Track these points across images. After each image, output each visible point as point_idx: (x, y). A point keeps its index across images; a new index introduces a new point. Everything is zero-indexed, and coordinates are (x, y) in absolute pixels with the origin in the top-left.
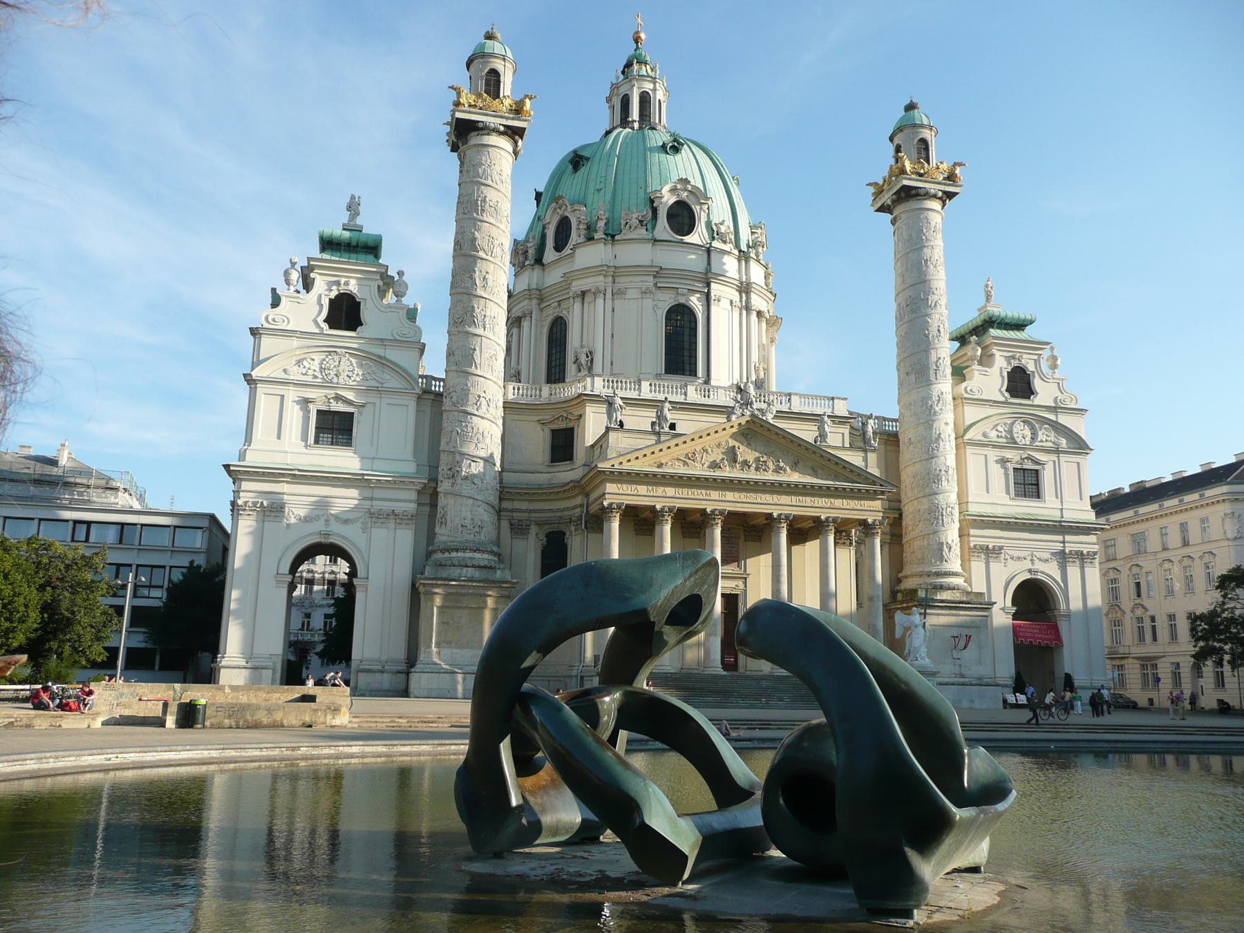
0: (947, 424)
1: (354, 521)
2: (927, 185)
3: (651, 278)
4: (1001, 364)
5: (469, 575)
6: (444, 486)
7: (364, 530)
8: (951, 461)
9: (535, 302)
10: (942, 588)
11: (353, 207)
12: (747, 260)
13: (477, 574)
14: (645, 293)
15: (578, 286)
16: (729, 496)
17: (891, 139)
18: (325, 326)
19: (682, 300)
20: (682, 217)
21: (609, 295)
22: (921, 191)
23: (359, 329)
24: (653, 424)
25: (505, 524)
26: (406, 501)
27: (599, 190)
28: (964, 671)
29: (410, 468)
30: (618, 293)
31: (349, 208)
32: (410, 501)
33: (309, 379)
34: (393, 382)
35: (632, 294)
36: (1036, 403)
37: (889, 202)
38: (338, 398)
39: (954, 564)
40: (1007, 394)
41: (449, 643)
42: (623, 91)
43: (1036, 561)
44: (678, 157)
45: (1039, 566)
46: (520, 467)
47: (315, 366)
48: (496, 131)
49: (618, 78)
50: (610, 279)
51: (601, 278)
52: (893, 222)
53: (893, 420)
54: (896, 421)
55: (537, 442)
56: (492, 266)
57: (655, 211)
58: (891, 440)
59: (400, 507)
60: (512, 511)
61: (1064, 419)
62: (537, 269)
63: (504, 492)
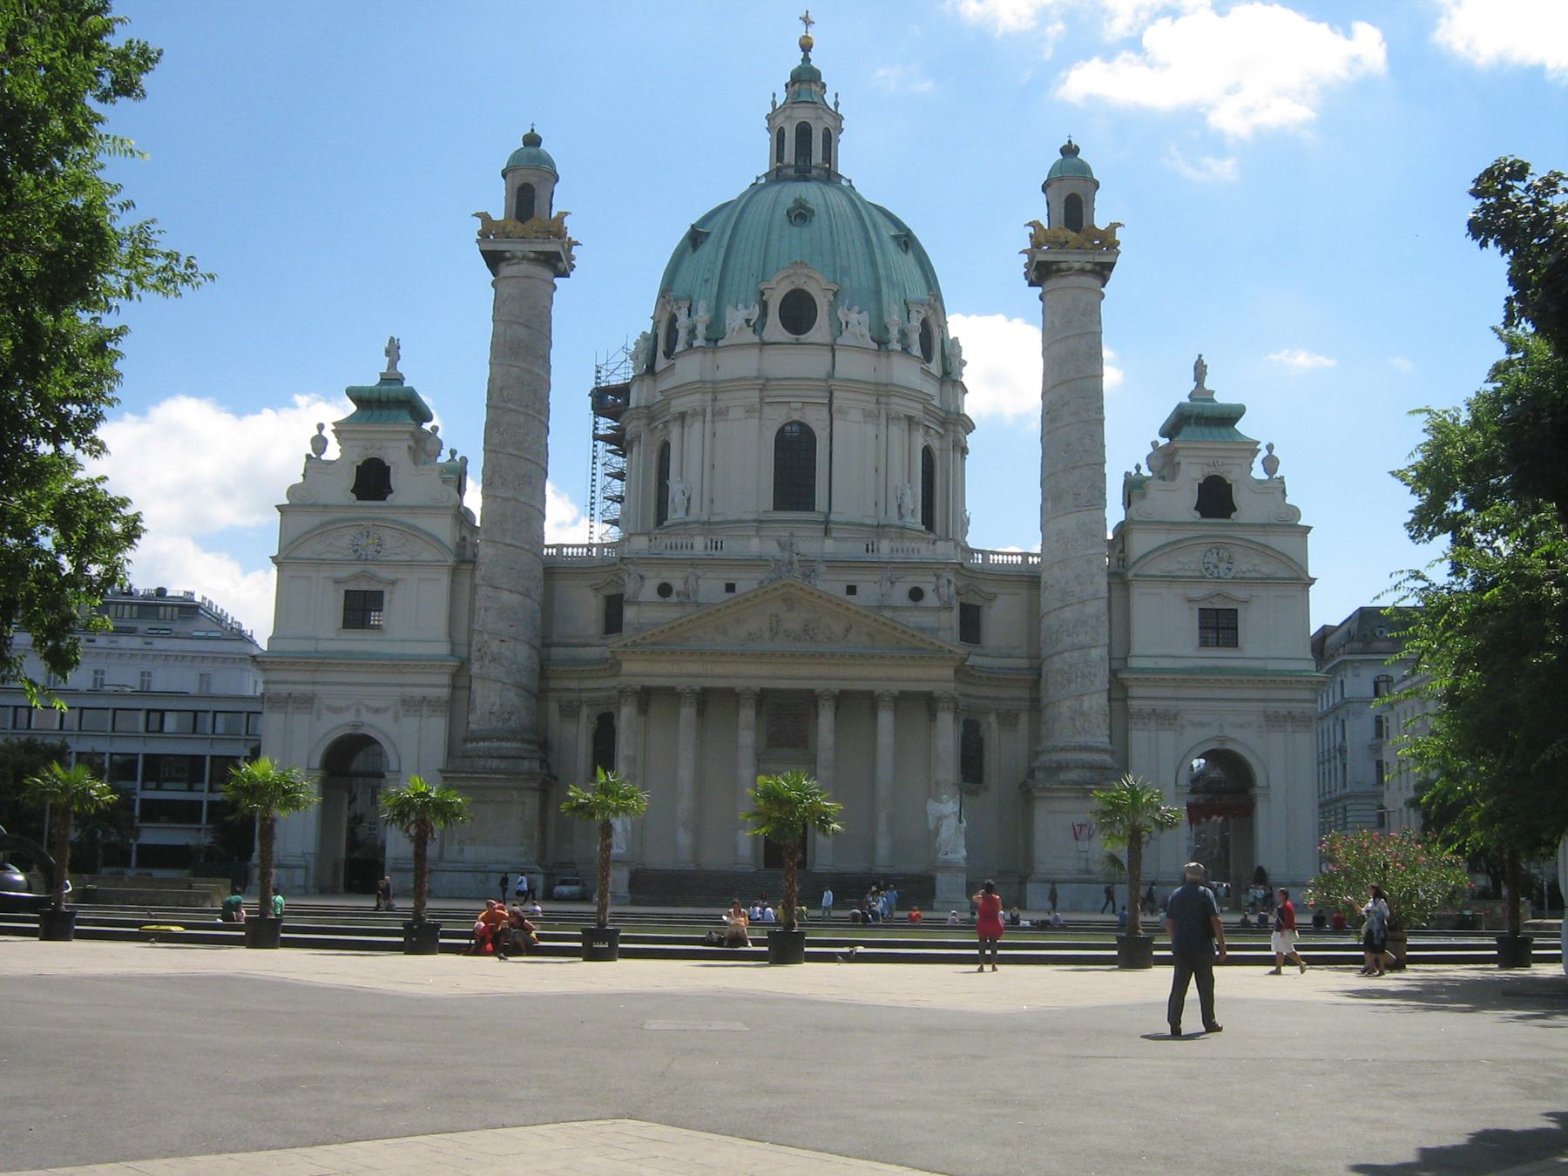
0: (1089, 562)
1: (386, 710)
2: (1069, 258)
3: (757, 393)
4: (1192, 475)
6: (475, 668)
7: (396, 719)
8: (1097, 607)
9: (643, 422)
11: (393, 351)
13: (503, 765)
14: (749, 411)
15: (678, 405)
16: (765, 670)
17: (1044, 189)
18: (354, 497)
19: (796, 416)
20: (798, 312)
21: (708, 417)
22: (1063, 266)
23: (390, 497)
25: (553, 707)
26: (437, 686)
27: (706, 281)
29: (443, 649)
30: (720, 414)
31: (388, 353)
32: (443, 686)
33: (338, 556)
34: (428, 554)
35: (736, 413)
39: (1101, 738)
40: (1198, 514)
42: (779, 122)
45: (1228, 732)
46: (574, 641)
47: (345, 542)
48: (525, 258)
49: (774, 103)
50: (709, 397)
51: (698, 396)
52: (1041, 298)
53: (1033, 555)
54: (1038, 555)
55: (585, 610)
56: (522, 418)
57: (764, 306)
62: (648, 381)
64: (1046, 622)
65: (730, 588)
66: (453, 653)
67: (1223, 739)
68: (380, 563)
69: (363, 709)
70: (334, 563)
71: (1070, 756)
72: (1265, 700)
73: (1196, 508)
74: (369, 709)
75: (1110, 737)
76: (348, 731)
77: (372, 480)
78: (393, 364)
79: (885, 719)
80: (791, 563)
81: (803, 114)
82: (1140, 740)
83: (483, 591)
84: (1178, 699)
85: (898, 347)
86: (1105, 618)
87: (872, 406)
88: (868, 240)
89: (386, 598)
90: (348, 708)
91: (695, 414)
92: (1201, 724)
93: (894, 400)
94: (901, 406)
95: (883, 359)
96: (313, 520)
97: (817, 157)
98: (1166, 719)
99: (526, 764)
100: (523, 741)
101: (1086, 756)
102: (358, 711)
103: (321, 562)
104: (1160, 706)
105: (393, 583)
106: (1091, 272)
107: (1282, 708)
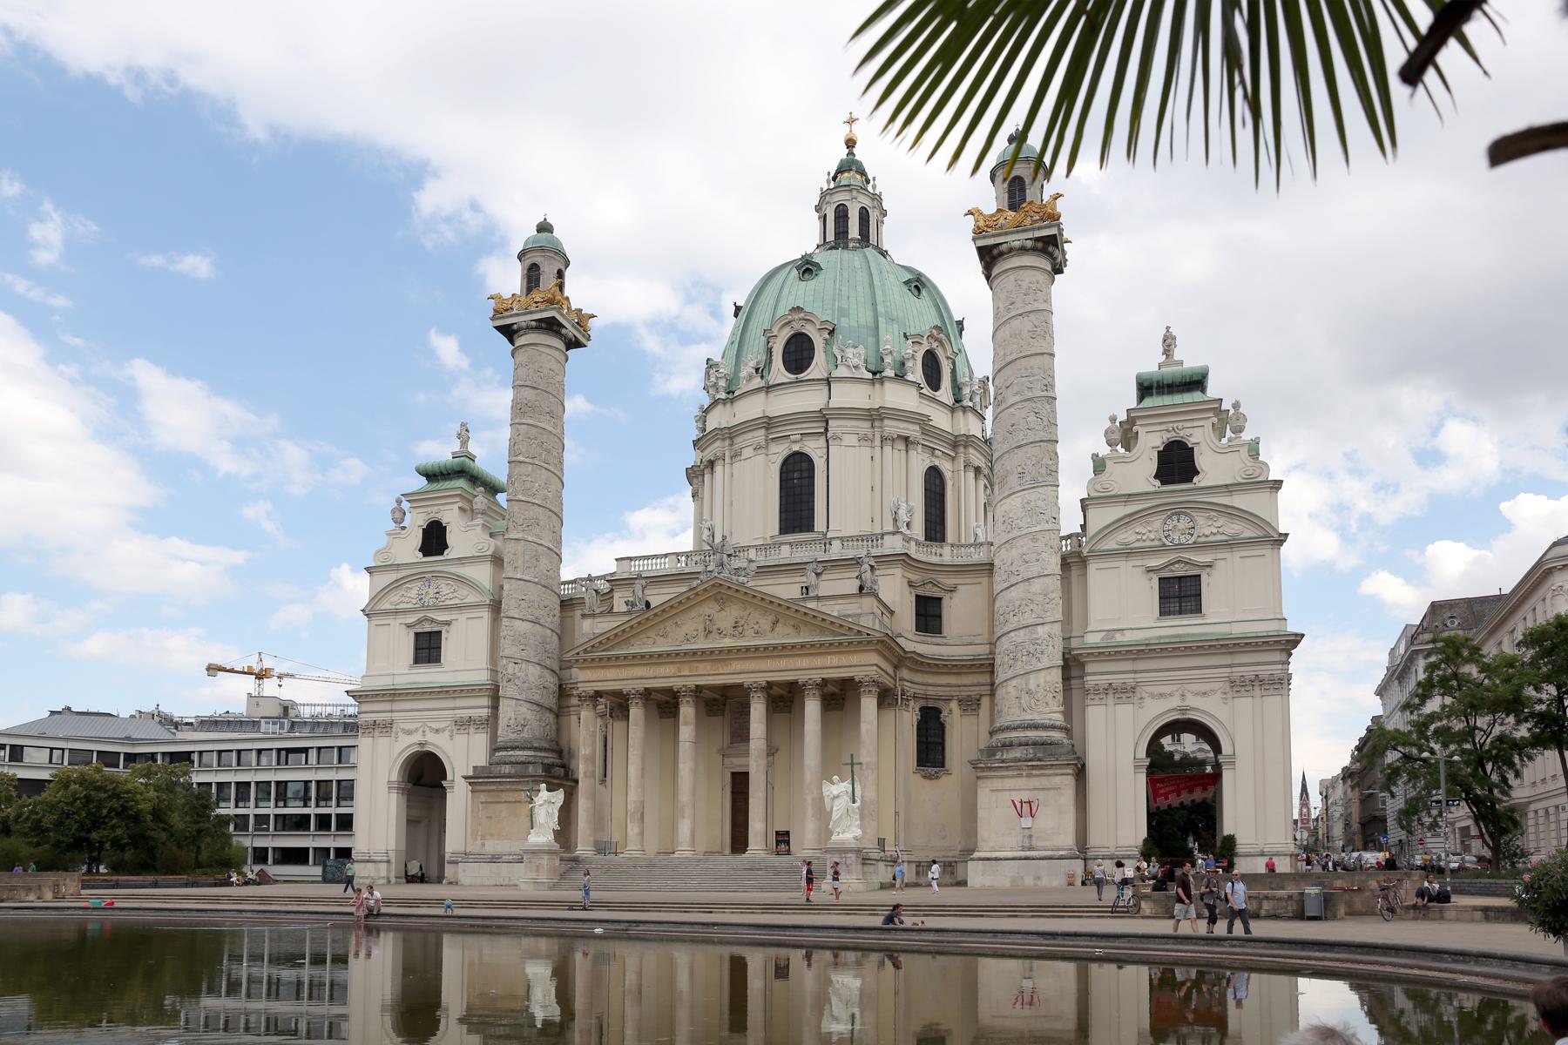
3: (762, 432)
10: (1011, 745)
12: (882, 381)
15: (709, 454)
16: (704, 668)
19: (796, 448)
20: (798, 353)
26: (479, 707)
30: (736, 455)
31: (459, 436)
35: (747, 452)
38: (426, 619)
43: (1189, 696)
44: (811, 285)
45: (1191, 701)
47: (413, 593)
50: (727, 442)
51: (718, 443)
57: (770, 351)
58: (988, 568)
63: (563, 692)
64: (997, 604)
67: (1183, 710)
70: (406, 612)
71: (1014, 734)
75: (1067, 714)
77: (434, 539)
78: (464, 443)
79: (812, 708)
80: (722, 565)
81: (841, 197)
83: (505, 622)
84: (1135, 672)
85: (889, 373)
86: (1057, 595)
87: (869, 432)
88: (872, 285)
89: (444, 635)
91: (718, 458)
92: (1162, 695)
93: (886, 422)
94: (893, 427)
95: (877, 386)
96: (393, 576)
97: (854, 231)
98: (1125, 692)
99: (531, 768)
100: (536, 749)
101: (1032, 734)
103: (396, 612)
104: (1117, 680)
105: (448, 623)
107: (1249, 672)
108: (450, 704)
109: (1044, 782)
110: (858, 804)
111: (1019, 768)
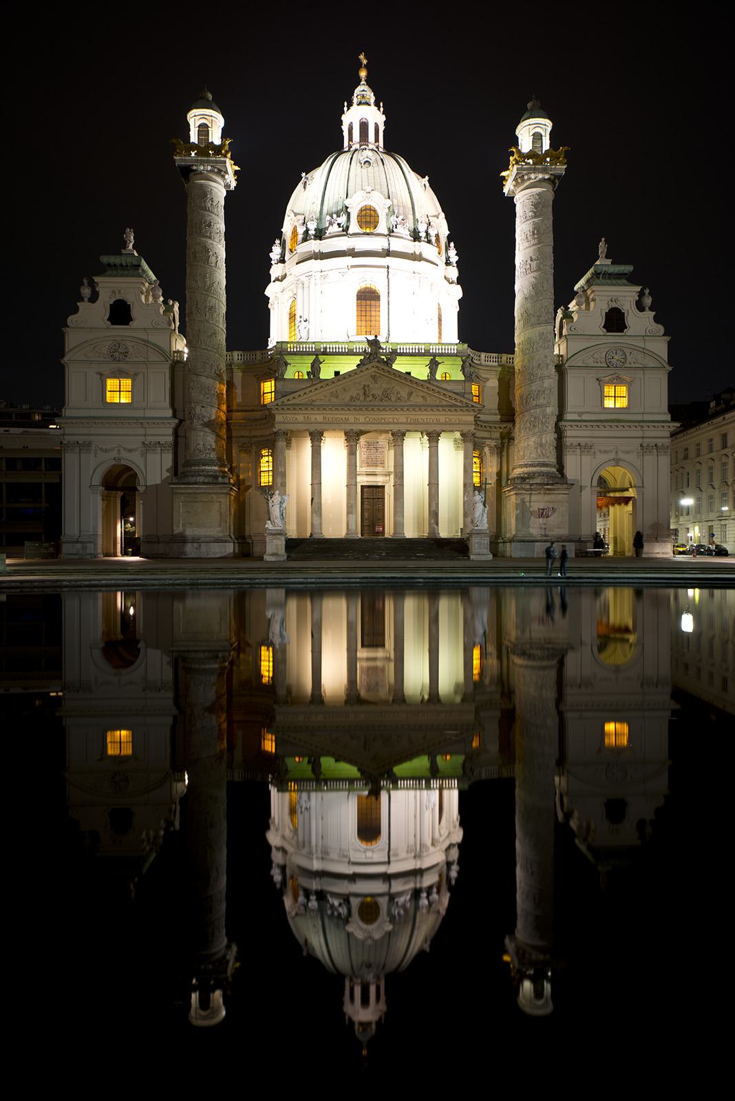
5: (201, 481)
6: (188, 422)
24: (308, 373)
26: (166, 435)
28: (547, 533)
29: (169, 413)
33: (103, 359)
36: (627, 334)
37: (512, 188)
40: (605, 330)
41: (191, 524)
45: (621, 456)
59: (163, 440)
60: (238, 437)
61: (649, 346)
65: (337, 373)
66: (174, 416)
68: (127, 362)
69: (122, 449)
72: (642, 438)
73: (604, 327)
74: (125, 449)
76: (114, 463)
82: (570, 461)
90: (112, 449)
98: (585, 448)
102: (119, 451)
104: (583, 441)
106: (549, 179)
108: (142, 431)
109: (552, 497)
110: (486, 509)
111: (540, 489)
